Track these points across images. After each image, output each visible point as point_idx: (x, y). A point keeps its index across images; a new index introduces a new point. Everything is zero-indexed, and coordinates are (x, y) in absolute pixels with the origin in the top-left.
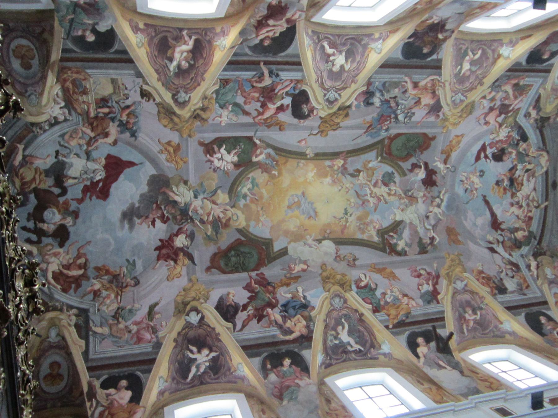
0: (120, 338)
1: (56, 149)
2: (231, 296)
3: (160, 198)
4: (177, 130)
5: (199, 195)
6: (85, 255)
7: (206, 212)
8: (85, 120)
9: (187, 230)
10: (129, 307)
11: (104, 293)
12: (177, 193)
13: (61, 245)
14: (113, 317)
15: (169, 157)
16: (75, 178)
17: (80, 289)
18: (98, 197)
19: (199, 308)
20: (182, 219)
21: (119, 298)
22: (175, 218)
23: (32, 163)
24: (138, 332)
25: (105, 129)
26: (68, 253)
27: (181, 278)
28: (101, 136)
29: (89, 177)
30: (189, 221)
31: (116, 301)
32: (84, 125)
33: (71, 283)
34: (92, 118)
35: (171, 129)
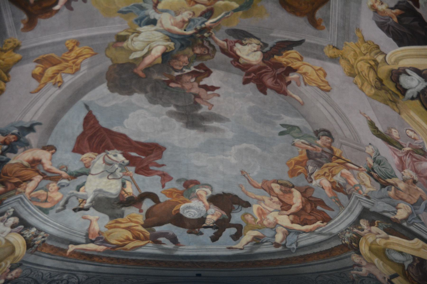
0: (421, 199)
1: (73, 212)
2: (381, 8)
3: (156, 76)
4: (7, 72)
5: (148, 16)
6: (265, 182)
7: (186, 6)
8: (12, 193)
9: (226, 41)
10: (370, 161)
11: (338, 178)
12: (146, 51)
13: (248, 205)
14: (383, 186)
15: (68, 70)
16: (124, 185)
17: (327, 203)
18: (160, 156)
19: (396, 67)
20: (202, 46)
21: (349, 165)
22: (198, 57)
23: (100, 233)
24: (416, 172)
25: (25, 167)
26: (259, 201)
27: (328, 72)
28: (39, 167)
29: (120, 169)
30: (206, 35)
31: (356, 172)
32: (20, 193)
33: (314, 209)
34: (6, 187)
35: (5, 82)
